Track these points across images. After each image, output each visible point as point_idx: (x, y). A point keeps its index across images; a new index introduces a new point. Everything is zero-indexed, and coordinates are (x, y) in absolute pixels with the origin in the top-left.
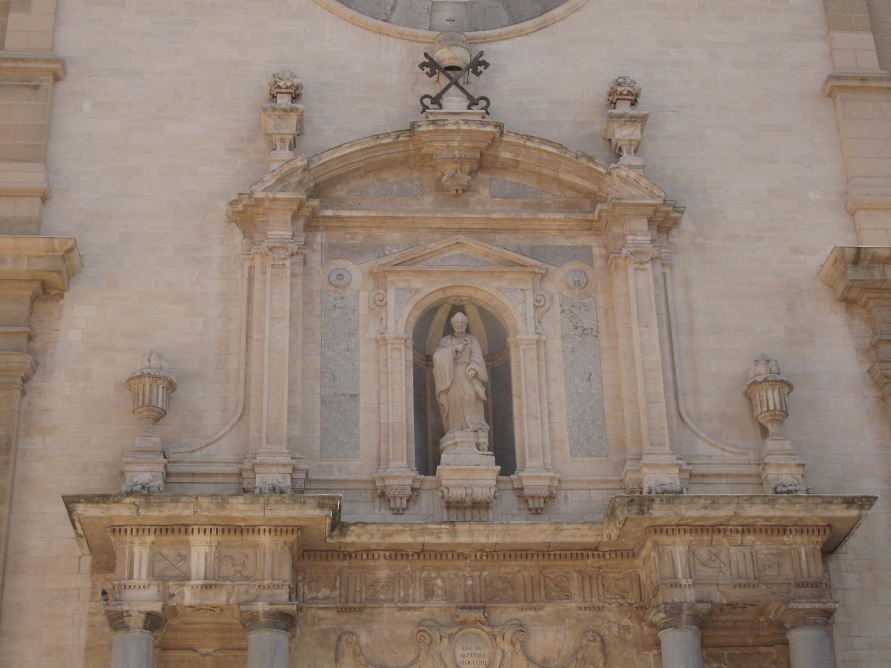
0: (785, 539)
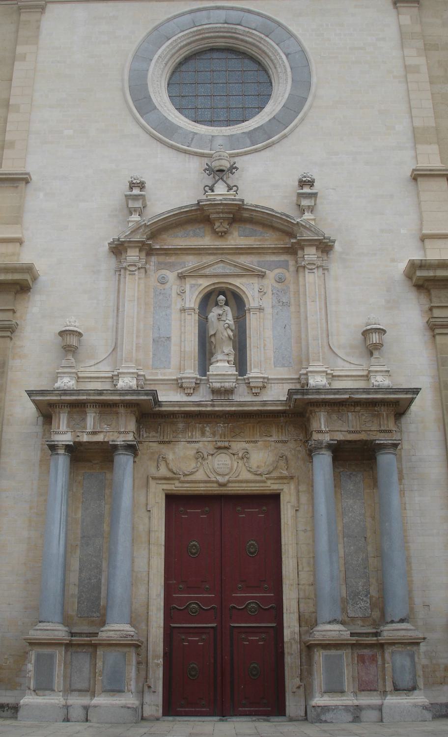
0: (376, 409)
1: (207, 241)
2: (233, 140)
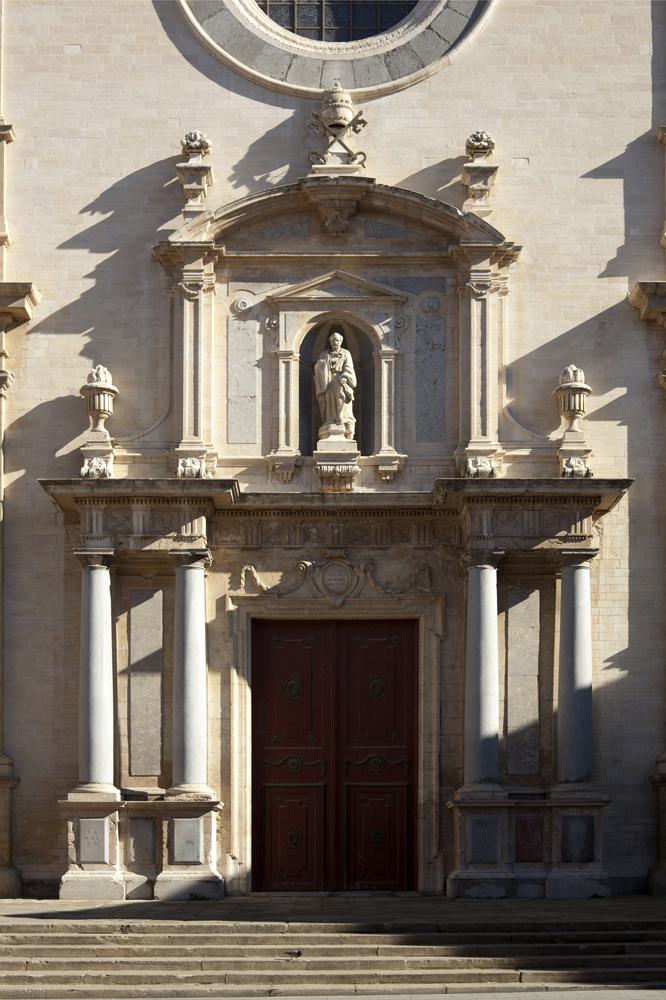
1: (310, 248)
2: (356, 71)
